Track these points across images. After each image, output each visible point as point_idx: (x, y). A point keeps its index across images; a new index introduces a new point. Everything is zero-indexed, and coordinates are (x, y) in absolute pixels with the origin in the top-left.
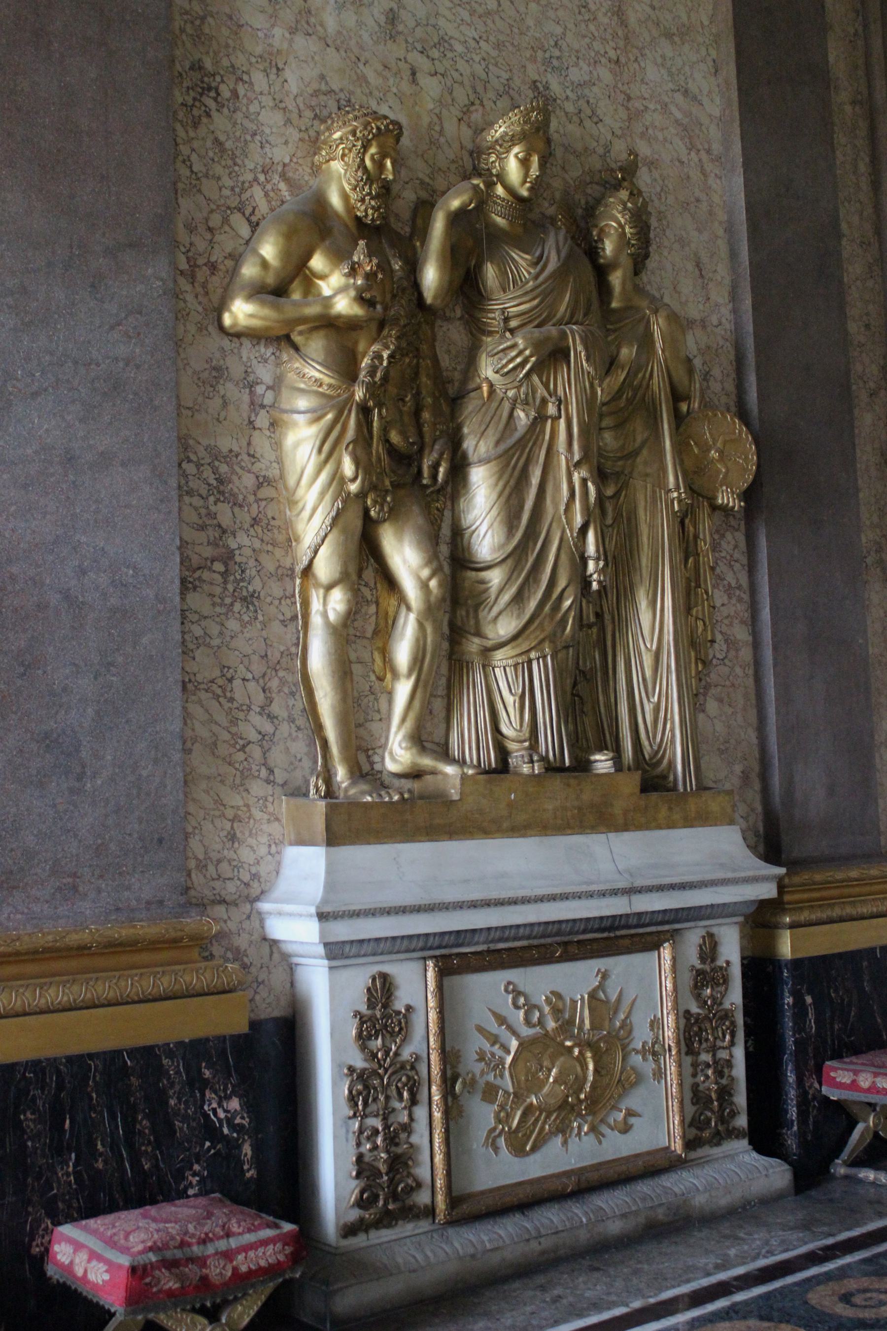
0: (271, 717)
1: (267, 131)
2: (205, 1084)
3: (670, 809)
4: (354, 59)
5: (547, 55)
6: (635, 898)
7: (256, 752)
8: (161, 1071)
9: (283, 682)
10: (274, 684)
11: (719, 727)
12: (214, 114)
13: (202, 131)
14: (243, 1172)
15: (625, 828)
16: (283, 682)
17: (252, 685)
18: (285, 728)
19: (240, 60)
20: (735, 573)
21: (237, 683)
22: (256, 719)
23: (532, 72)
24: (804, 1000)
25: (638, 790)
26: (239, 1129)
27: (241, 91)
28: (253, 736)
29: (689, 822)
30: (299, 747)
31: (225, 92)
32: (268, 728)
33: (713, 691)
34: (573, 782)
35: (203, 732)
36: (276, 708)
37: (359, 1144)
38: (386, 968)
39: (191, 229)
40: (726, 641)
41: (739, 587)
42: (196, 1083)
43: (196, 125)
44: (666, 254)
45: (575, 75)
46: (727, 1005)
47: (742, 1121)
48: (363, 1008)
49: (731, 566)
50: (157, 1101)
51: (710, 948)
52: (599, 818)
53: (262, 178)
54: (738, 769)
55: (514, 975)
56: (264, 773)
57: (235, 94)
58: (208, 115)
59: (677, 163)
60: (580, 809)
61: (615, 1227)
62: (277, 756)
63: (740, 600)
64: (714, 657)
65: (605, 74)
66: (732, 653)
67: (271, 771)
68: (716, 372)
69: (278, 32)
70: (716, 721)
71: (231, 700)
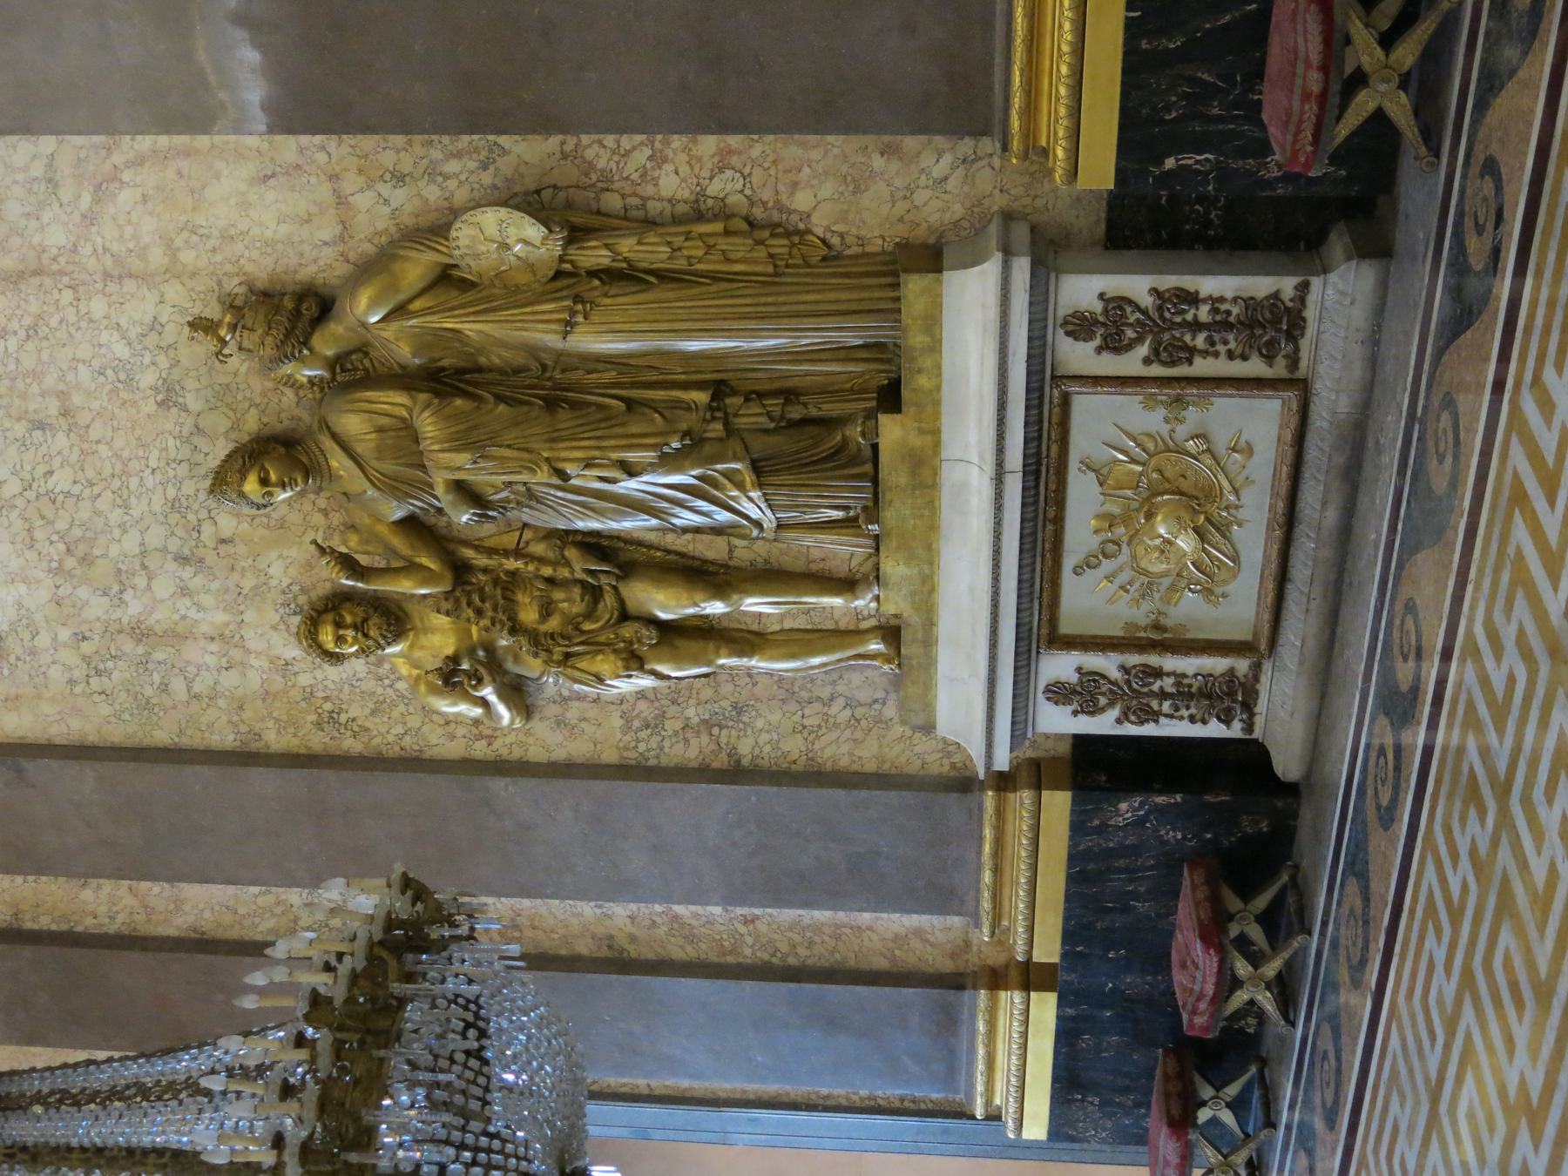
0: (832, 699)
1: (344, 676)
2: (1104, 825)
3: (920, 371)
4: (241, 598)
5: (120, 386)
6: (1008, 466)
7: (859, 712)
8: (1088, 850)
9: (802, 688)
10: (805, 695)
11: (827, 190)
12: (352, 715)
13: (368, 724)
14: (1176, 804)
15: (936, 432)
16: (802, 688)
17: (807, 712)
18: (840, 688)
19: (296, 694)
20: (634, 148)
21: (806, 722)
22: (833, 710)
23: (150, 407)
24: (1171, 170)
25: (897, 417)
26: (1142, 805)
27: (321, 694)
28: (848, 712)
29: (935, 347)
30: (856, 678)
31: (328, 706)
32: (841, 702)
33: (784, 198)
34: (888, 496)
35: (845, 748)
36: (825, 694)
37: (1182, 718)
38: (1041, 687)
39: (452, 737)
40: (721, 170)
41: (652, 143)
42: (1102, 829)
43: (367, 730)
44: (269, 234)
45: (121, 350)
46: (1147, 301)
47: (1287, 285)
48: (1070, 709)
49: (627, 154)
50: (1109, 854)
51: (1080, 326)
52: (925, 465)
53: (387, 682)
54: (878, 162)
55: (1069, 563)
56: (877, 706)
57: (326, 699)
58: (354, 720)
59: (149, 205)
60: (914, 488)
61: (1332, 516)
62: (864, 696)
63: (667, 143)
64: (741, 192)
65: (98, 307)
66: (735, 161)
67: (876, 701)
68: (388, 159)
69: (255, 662)
70: (820, 197)
71: (819, 726)
